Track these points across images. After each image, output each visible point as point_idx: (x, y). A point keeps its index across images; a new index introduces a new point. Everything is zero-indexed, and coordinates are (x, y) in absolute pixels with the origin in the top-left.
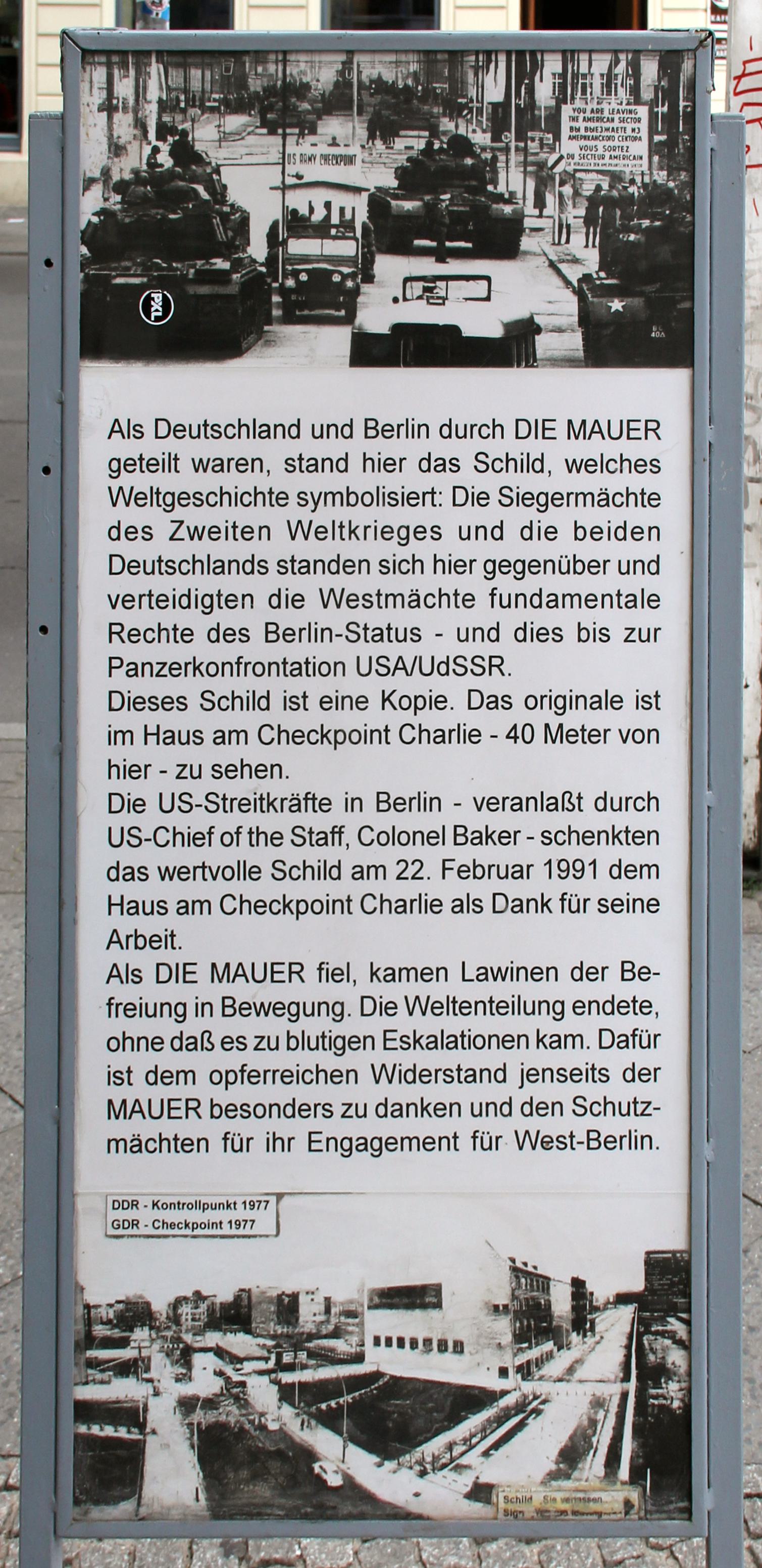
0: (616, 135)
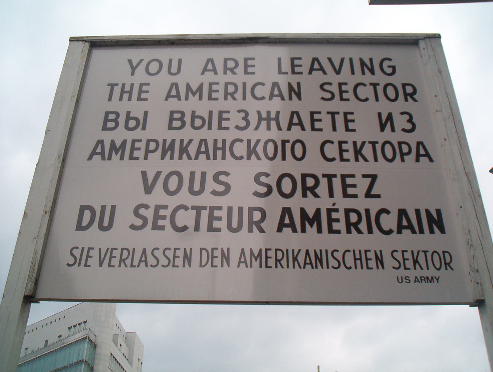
0: (313, 141)
